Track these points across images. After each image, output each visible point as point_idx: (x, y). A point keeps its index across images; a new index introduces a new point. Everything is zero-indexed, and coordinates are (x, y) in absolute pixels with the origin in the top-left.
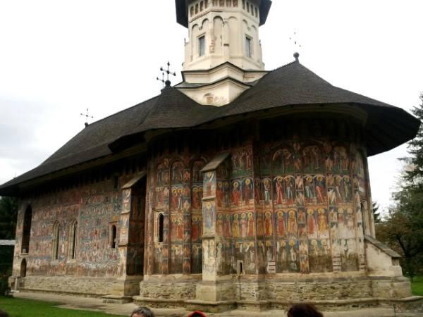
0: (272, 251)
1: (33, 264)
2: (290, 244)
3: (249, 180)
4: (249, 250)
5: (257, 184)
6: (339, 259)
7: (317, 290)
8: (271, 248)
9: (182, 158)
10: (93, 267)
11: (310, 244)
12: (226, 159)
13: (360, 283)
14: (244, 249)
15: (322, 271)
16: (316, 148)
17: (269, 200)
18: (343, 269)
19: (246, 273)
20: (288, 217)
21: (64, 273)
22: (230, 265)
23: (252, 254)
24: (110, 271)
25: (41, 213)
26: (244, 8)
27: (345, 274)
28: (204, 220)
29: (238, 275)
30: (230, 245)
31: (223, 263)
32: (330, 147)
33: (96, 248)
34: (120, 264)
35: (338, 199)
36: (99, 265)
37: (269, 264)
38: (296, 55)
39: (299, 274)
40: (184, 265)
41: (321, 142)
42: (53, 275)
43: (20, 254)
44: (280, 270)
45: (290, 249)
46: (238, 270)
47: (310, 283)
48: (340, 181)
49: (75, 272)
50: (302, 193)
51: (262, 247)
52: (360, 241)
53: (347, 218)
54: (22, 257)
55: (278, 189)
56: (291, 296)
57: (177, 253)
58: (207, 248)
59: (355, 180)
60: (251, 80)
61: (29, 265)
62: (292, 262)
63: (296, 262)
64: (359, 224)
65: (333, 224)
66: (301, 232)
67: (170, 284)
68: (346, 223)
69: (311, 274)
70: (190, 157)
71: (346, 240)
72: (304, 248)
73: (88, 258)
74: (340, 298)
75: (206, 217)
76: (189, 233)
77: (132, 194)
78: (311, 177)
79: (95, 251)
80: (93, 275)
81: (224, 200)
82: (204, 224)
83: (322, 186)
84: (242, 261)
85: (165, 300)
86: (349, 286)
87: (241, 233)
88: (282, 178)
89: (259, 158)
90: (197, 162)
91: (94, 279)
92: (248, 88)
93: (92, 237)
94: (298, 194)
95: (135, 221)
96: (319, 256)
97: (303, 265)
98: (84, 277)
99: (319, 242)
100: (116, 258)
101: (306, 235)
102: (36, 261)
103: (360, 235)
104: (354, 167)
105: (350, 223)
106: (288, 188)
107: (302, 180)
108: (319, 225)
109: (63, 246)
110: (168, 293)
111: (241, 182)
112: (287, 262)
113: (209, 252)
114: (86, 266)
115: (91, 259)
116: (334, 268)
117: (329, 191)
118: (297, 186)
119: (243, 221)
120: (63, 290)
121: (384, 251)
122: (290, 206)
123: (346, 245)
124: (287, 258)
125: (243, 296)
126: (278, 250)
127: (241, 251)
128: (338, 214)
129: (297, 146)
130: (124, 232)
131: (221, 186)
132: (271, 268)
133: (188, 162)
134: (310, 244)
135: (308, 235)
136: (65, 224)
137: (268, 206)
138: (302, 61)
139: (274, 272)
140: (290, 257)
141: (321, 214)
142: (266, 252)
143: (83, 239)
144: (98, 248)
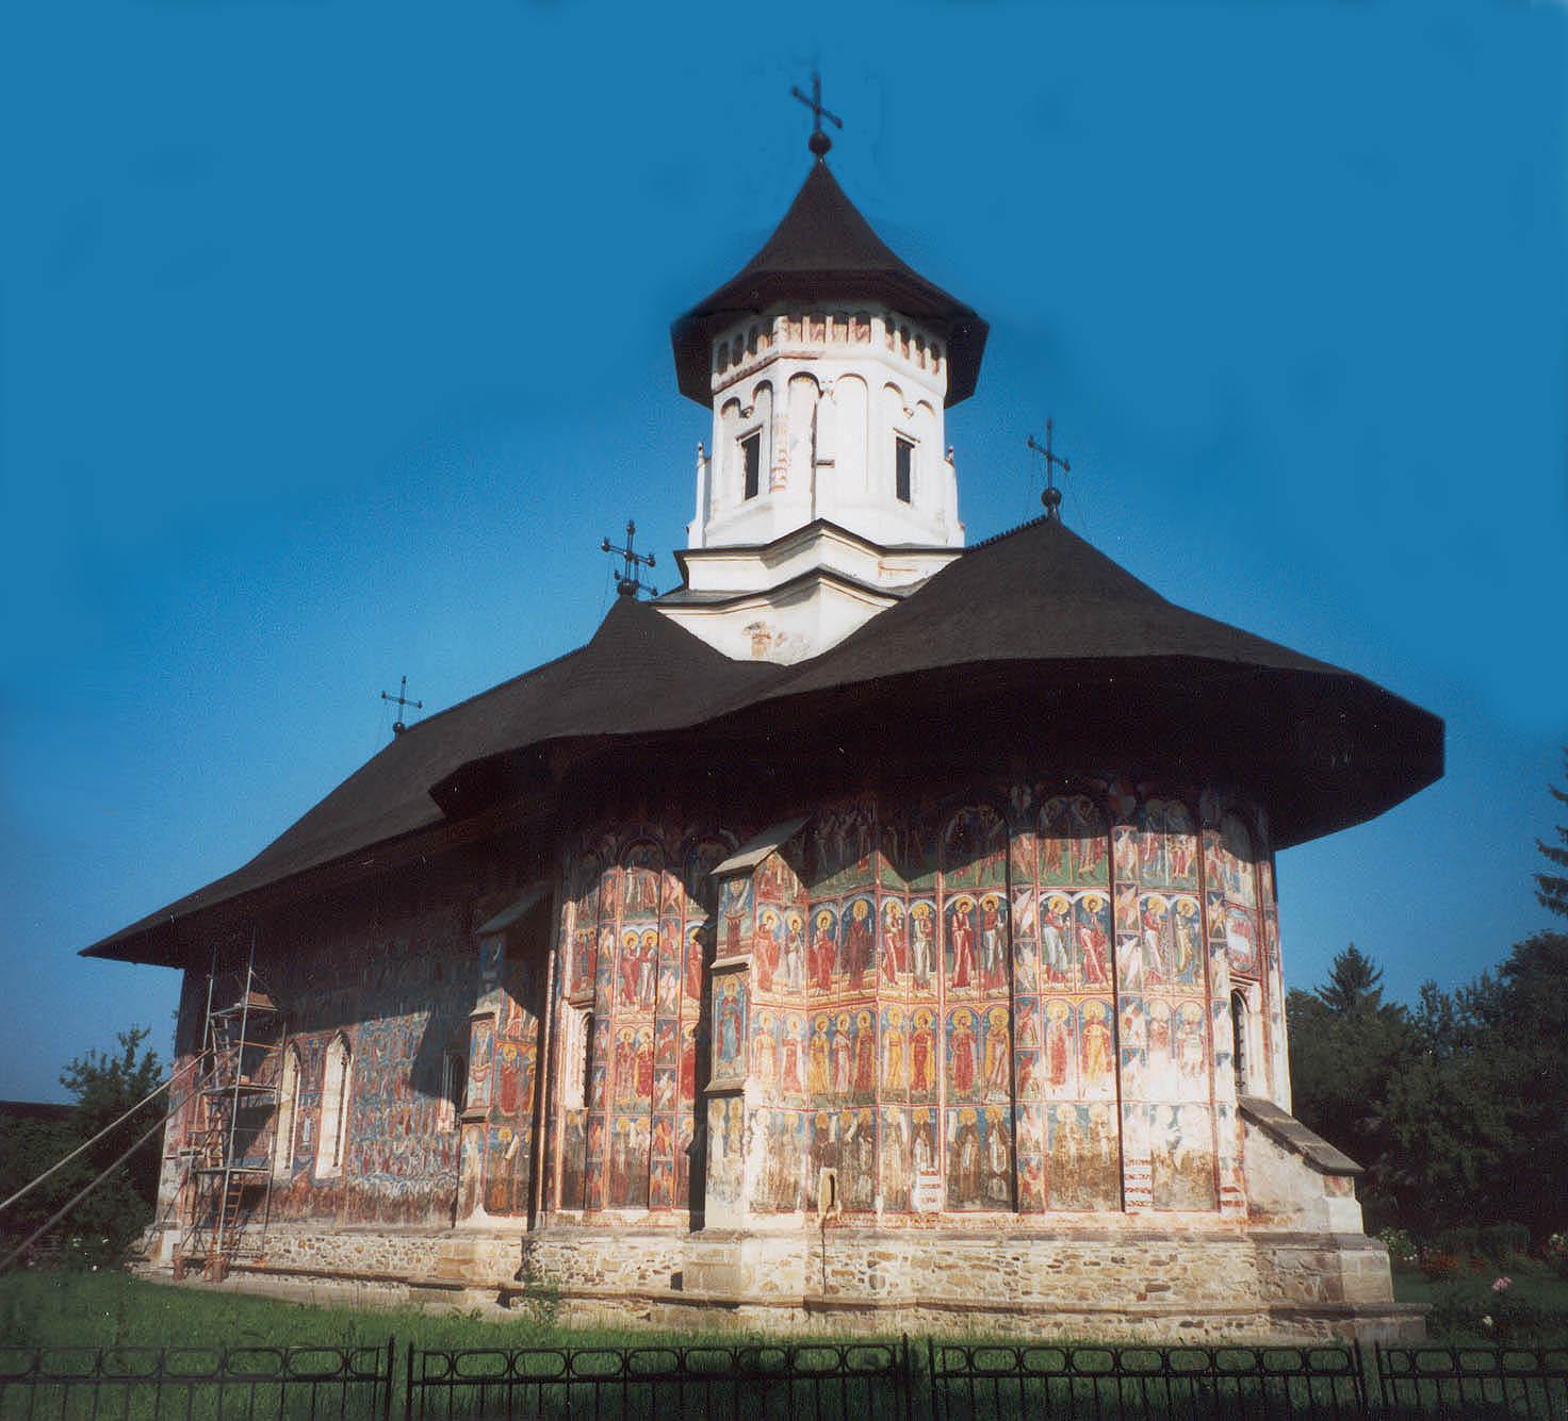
0: (932, 1144)
2: (987, 1116)
3: (864, 906)
4: (857, 1135)
5: (889, 920)
6: (1148, 1170)
7: (1067, 1264)
8: (928, 1132)
9: (660, 832)
10: (393, 1191)
11: (1052, 1119)
12: (798, 836)
13: (1216, 1249)
14: (839, 1139)
15: (1091, 1208)
16: (1085, 804)
17: (929, 974)
18: (1160, 1204)
19: (845, 1211)
20: (987, 1029)
21: (307, 1210)
22: (796, 1183)
23: (865, 1147)
26: (891, 346)
27: (1161, 1221)
28: (715, 1037)
29: (822, 1214)
30: (800, 1120)
31: (771, 1175)
32: (1132, 800)
33: (401, 1129)
34: (465, 1178)
35: (1153, 977)
36: (409, 1183)
37: (921, 1180)
38: (1051, 498)
39: (1012, 1216)
40: (652, 1180)
41: (1104, 784)
44: (956, 1202)
45: (988, 1135)
46: (823, 1200)
47: (1045, 1244)
48: (1161, 912)
49: (341, 1207)
50: (1034, 948)
51: (898, 1126)
52: (1223, 1112)
53: (1180, 1035)
55: (959, 936)
56: (983, 1283)
57: (633, 1142)
58: (722, 1123)
59: (1214, 912)
60: (884, 582)
62: (992, 1175)
63: (1003, 1175)
64: (1220, 1057)
65: (1131, 1053)
66: (1024, 1079)
67: (609, 1239)
68: (1177, 1051)
69: (1049, 1215)
70: (684, 829)
71: (1175, 1109)
72: (1033, 1130)
74: (1142, 1297)
75: (721, 1023)
76: (671, 1078)
77: (510, 953)
78: (1066, 897)
79: (398, 1138)
80: (392, 1219)
81: (782, 968)
82: (715, 1046)
83: (1101, 928)
84: (834, 1171)
85: (589, 1287)
86: (1173, 1258)
87: (835, 1079)
88: (972, 900)
89: (901, 834)
90: (702, 847)
91: (395, 1231)
92: (891, 603)
94: (1019, 952)
95: (515, 1040)
96: (1081, 1158)
97: (1027, 1186)
98: (364, 1224)
99: (1083, 1113)
100: (458, 1159)
101: (1037, 1087)
103: (1227, 1094)
104: (1214, 868)
105: (1194, 1054)
106: (991, 934)
107: (1034, 906)
108: (1085, 1056)
109: (307, 1123)
110: (597, 1267)
111: (839, 913)
112: (978, 1174)
113: (726, 1138)
114: (373, 1185)
115: (386, 1166)
116: (1128, 1196)
117: (1121, 944)
118: (1018, 925)
119: (840, 1040)
120: (296, 1266)
121: (1293, 1149)
122: (994, 992)
123: (1171, 1126)
124: (978, 1163)
125: (832, 1281)
126: (951, 1138)
127: (832, 1139)
128: (1148, 1023)
129: (1020, 797)
130: (481, 1074)
131: (772, 925)
132: (929, 1193)
133: (679, 844)
134: (1052, 1119)
135: (1048, 1087)
136: (315, 1052)
137: (923, 994)
138: (1068, 518)
139: (938, 1206)
140: (988, 1158)
141: (1090, 1023)
142: (914, 1142)
143: (366, 1101)
144: (408, 1130)
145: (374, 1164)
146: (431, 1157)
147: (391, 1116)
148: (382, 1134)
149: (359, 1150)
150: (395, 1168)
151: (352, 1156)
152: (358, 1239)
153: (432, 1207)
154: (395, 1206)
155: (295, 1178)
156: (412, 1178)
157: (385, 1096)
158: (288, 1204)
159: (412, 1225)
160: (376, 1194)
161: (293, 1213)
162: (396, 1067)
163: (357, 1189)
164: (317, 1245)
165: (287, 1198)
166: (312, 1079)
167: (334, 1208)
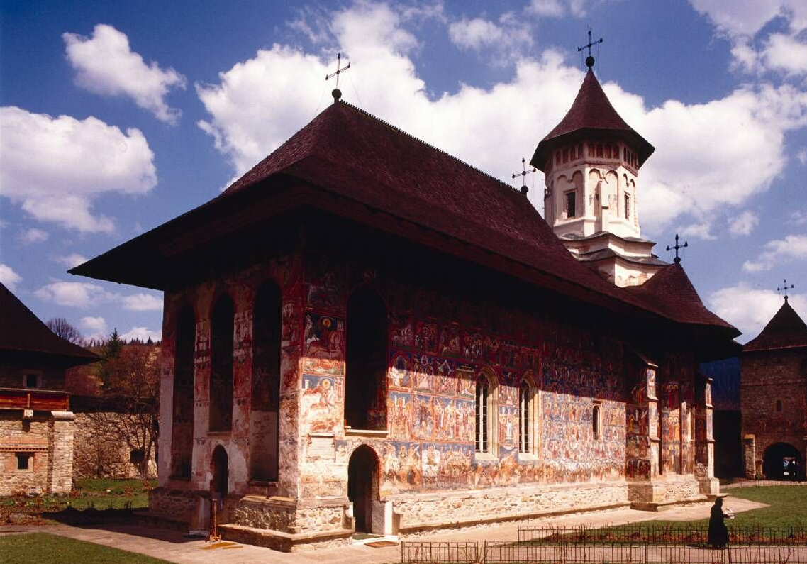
1: (410, 462)
10: (572, 467)
21: (515, 479)
24: (597, 473)
25: (430, 332)
33: (574, 436)
36: (580, 464)
42: (488, 485)
43: (339, 429)
54: (354, 442)
61: (389, 462)
73: (563, 452)
79: (573, 441)
80: (573, 481)
93: (567, 417)
102: (425, 454)
109: (509, 425)
115: (567, 455)
144: (578, 437)
145: (560, 453)
146: (590, 452)
147: (567, 429)
148: (563, 438)
149: (550, 446)
150: (572, 456)
151: (546, 448)
152: (562, 493)
153: (592, 474)
154: (574, 474)
155: (503, 460)
156: (581, 461)
157: (564, 419)
158: (498, 475)
159: (583, 483)
160: (563, 469)
161: (503, 481)
162: (568, 405)
163: (551, 466)
164: (536, 498)
165: (496, 473)
166: (509, 398)
167: (536, 477)
